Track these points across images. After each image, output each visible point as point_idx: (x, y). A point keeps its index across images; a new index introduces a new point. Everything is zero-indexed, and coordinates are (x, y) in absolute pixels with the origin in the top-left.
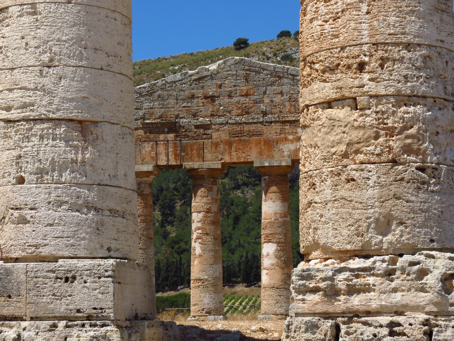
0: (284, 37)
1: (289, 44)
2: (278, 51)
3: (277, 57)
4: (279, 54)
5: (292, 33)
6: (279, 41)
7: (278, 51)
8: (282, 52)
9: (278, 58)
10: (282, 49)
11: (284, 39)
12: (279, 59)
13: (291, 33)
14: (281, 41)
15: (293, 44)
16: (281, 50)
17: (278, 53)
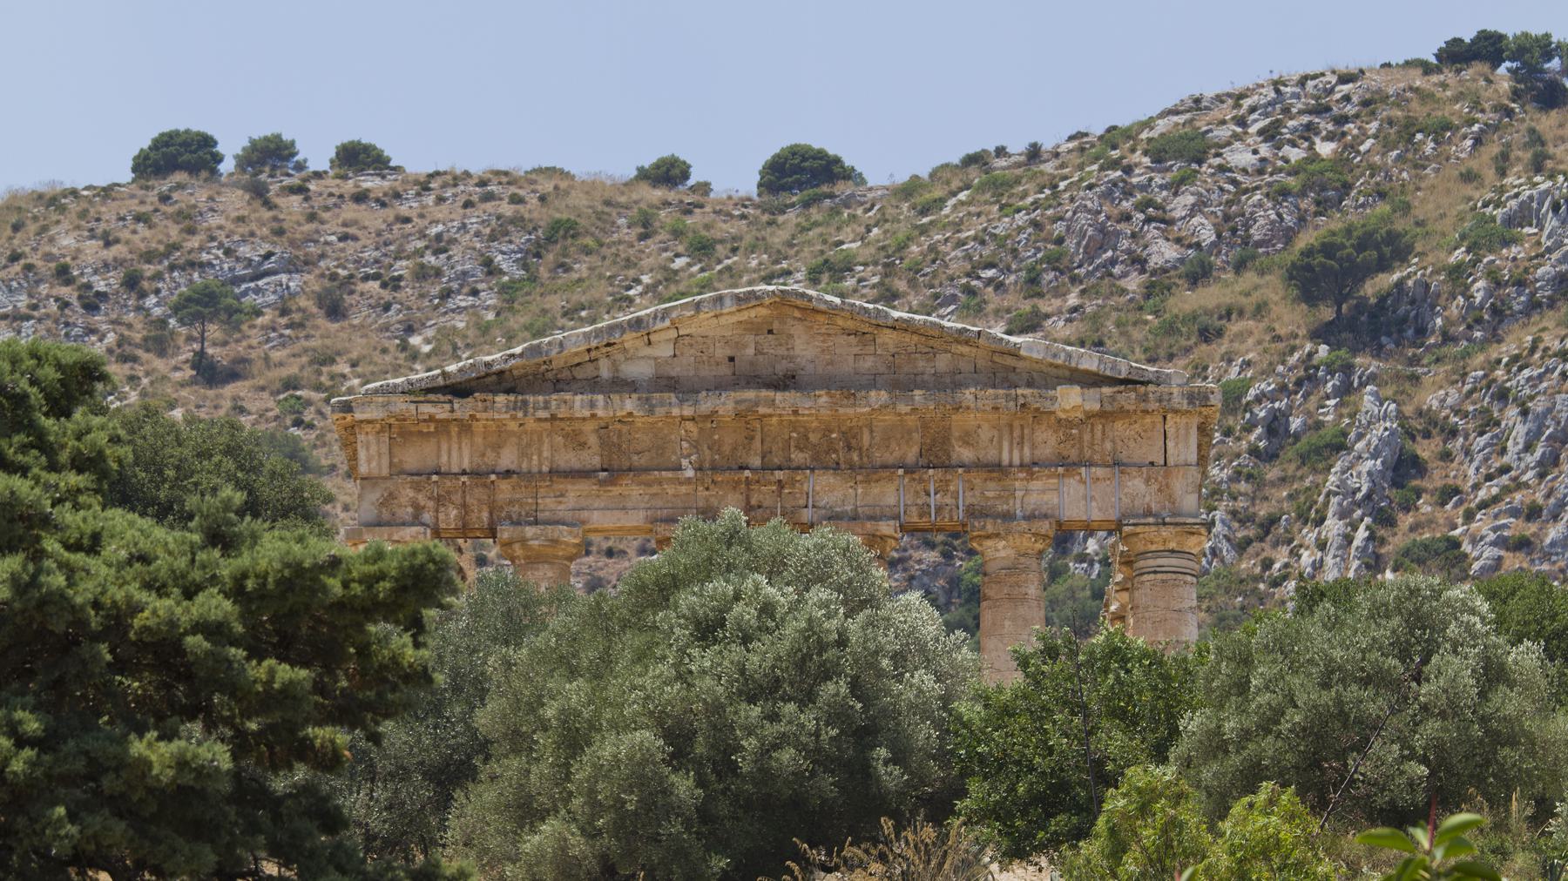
0: (180, 177)
1: (214, 221)
2: (149, 257)
3: (143, 295)
4: (158, 276)
5: (230, 147)
6: (152, 197)
7: (149, 257)
8: (172, 268)
9: (151, 300)
10: (175, 247)
11: (180, 186)
12: (158, 312)
13: (220, 148)
14: (165, 199)
15: (241, 219)
16: (166, 255)
17: (149, 269)
